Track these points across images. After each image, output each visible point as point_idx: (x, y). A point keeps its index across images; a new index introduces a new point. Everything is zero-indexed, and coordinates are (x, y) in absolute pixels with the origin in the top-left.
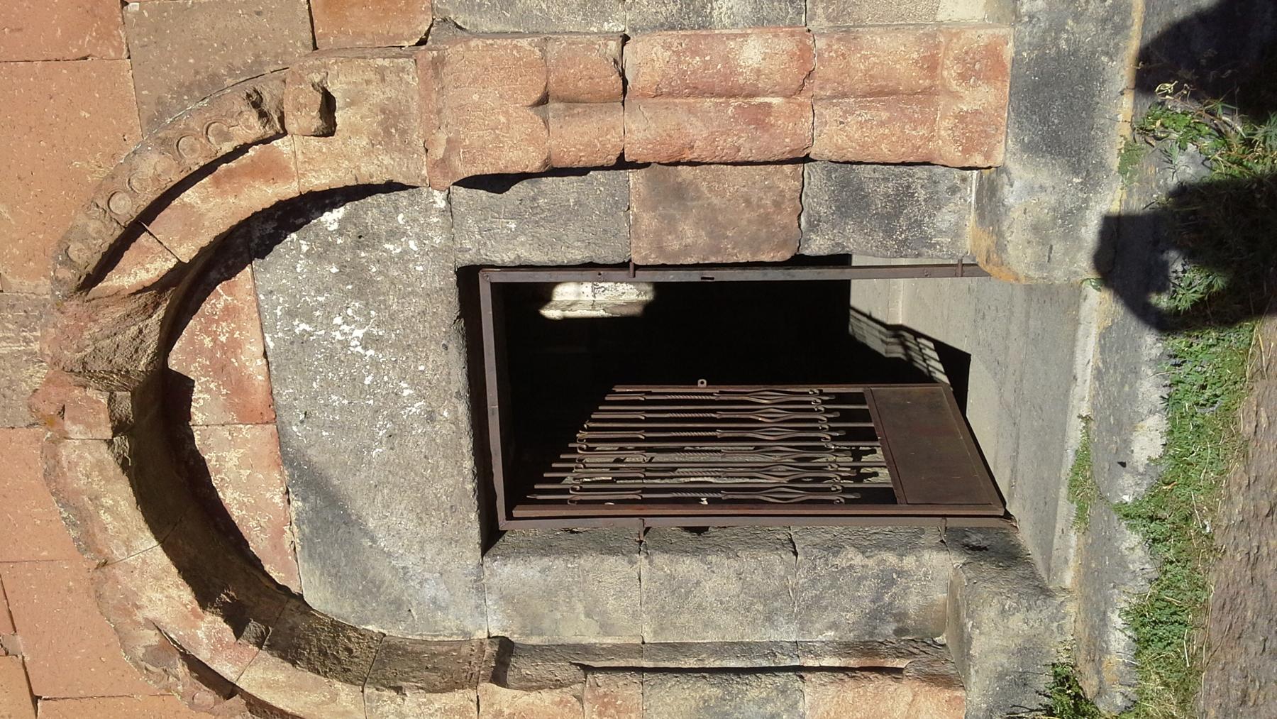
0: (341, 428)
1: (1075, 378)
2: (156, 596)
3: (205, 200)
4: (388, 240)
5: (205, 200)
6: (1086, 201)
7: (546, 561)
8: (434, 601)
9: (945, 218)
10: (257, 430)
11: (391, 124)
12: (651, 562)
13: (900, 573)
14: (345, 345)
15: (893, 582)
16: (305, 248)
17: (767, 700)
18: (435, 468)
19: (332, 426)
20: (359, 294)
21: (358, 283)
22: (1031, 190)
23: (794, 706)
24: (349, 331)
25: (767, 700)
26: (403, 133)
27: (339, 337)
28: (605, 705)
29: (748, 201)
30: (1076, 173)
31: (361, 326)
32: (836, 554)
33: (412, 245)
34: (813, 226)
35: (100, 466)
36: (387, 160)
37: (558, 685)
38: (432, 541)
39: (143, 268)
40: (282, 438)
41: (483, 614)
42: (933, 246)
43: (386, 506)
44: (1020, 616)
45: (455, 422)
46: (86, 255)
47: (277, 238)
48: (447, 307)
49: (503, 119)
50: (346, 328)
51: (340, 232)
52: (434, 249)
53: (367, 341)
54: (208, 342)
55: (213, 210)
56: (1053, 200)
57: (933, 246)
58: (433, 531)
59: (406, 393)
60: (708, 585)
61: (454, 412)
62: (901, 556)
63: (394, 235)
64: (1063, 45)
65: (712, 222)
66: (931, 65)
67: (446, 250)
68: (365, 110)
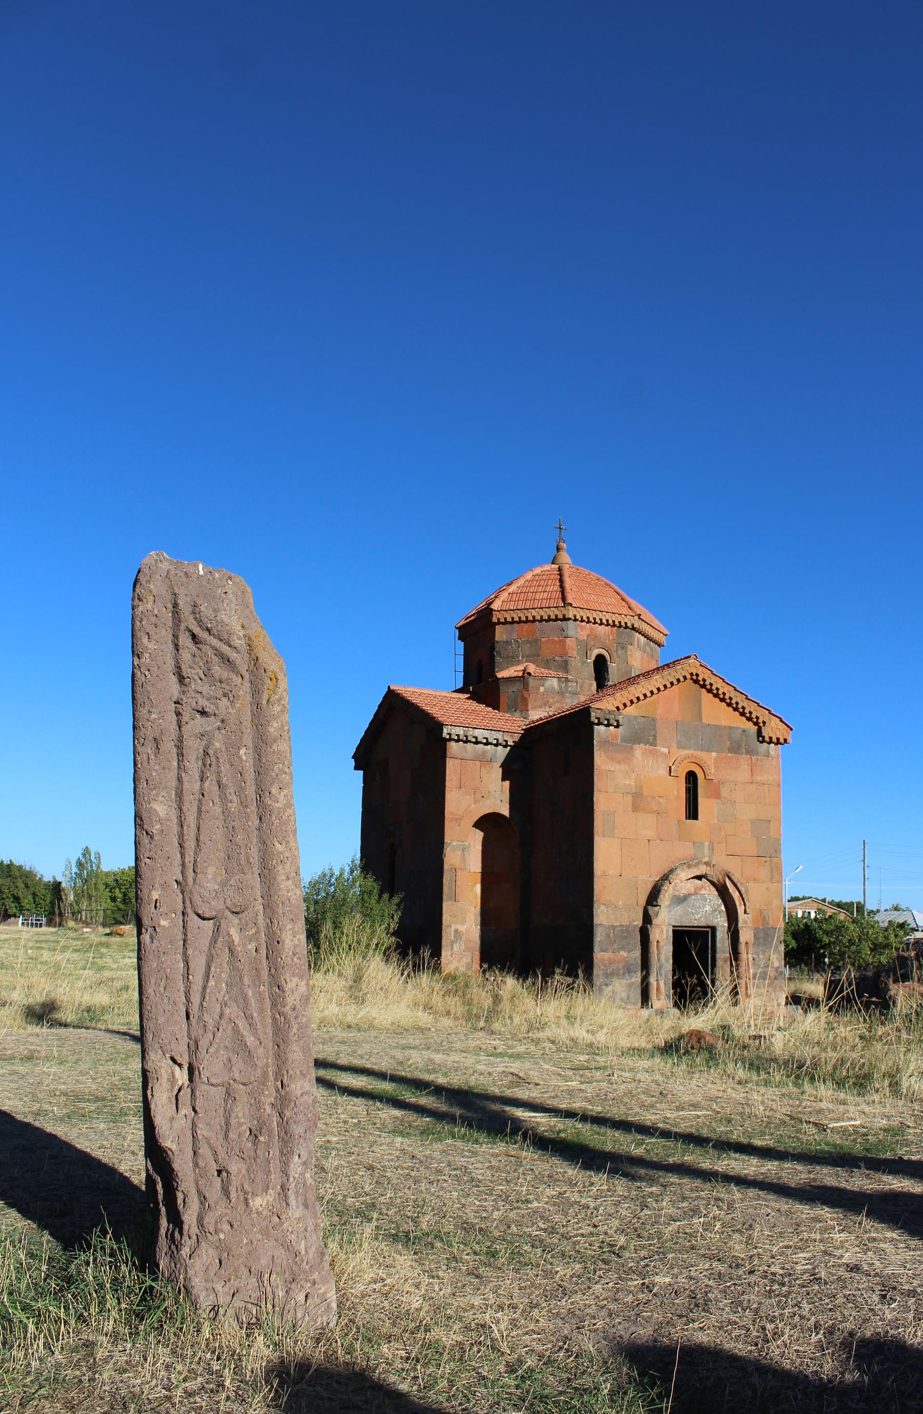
11: (746, 922)
21: (714, 911)
24: (708, 908)
46: (733, 878)
48: (711, 924)
55: (736, 895)
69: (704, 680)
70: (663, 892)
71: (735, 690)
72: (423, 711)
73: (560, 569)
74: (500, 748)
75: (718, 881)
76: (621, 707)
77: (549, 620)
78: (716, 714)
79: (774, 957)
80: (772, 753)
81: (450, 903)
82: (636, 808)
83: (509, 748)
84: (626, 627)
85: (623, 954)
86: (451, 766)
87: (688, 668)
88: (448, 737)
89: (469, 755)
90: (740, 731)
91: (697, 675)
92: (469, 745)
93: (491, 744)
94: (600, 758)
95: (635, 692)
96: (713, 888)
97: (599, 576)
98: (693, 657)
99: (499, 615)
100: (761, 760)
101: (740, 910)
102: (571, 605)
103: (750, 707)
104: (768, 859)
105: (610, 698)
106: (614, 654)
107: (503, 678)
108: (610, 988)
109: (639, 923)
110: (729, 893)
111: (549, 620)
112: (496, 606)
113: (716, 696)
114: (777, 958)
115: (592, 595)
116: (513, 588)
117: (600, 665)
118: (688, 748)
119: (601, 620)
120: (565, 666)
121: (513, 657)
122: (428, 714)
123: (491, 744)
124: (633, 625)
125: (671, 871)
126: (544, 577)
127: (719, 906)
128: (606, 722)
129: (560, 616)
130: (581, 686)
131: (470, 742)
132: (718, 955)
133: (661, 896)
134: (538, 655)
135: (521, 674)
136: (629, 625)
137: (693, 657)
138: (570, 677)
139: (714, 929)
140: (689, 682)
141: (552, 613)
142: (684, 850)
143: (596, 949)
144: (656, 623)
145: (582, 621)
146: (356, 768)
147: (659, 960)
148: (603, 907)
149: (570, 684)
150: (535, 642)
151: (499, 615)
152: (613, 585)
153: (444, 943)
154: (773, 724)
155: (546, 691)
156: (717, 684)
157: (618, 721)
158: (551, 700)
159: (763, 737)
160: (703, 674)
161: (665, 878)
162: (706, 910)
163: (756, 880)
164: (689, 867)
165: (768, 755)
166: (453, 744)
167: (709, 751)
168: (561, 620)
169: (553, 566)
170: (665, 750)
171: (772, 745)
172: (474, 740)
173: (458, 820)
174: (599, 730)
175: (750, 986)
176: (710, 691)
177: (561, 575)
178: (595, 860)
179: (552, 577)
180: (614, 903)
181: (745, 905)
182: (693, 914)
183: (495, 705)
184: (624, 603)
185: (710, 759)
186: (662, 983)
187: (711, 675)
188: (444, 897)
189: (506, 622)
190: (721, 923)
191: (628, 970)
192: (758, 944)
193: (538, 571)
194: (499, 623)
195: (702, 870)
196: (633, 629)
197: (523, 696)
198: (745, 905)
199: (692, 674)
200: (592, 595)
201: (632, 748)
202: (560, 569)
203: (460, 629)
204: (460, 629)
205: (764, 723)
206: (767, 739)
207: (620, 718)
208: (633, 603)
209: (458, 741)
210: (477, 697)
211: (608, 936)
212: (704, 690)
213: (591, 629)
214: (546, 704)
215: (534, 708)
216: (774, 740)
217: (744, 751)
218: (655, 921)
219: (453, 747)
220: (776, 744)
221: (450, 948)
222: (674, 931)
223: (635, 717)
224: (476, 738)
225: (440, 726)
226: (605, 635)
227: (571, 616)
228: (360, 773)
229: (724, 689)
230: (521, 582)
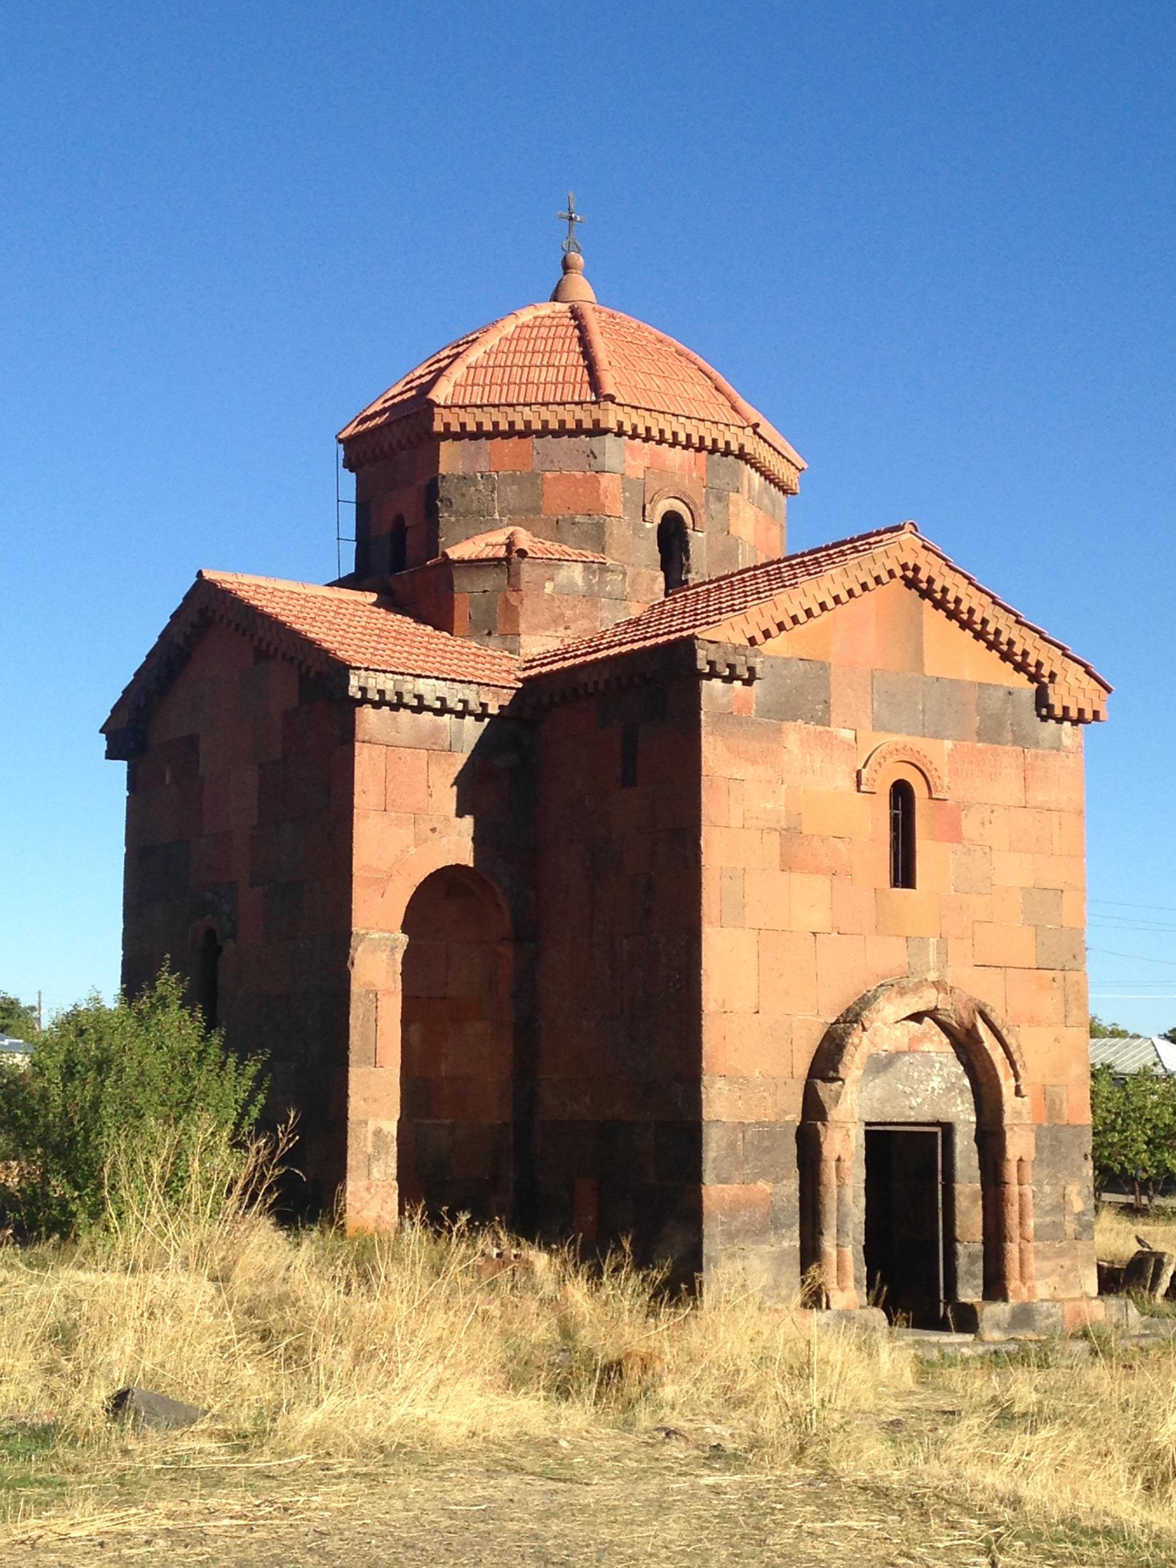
0: (907, 1075)
9: (970, 1292)
11: (1018, 1114)
20: (947, 1088)
22: (1004, 1312)
24: (936, 1082)
33: (960, 1108)
39: (983, 1029)
40: (904, 1053)
46: (992, 1016)
47: (962, 1063)
48: (943, 1118)
55: (997, 1054)
58: (876, 1105)
60: (855, 1210)
61: (913, 1116)
63: (963, 1102)
65: (966, 1213)
66: (1031, 1278)
69: (930, 581)
70: (849, 1049)
71: (995, 602)
72: (296, 633)
73: (576, 314)
74: (469, 719)
75: (961, 1024)
76: (760, 638)
77: (562, 431)
78: (955, 656)
79: (1073, 1190)
80: (1067, 741)
81: (364, 1069)
82: (787, 865)
83: (487, 720)
84: (727, 453)
85: (764, 1186)
86: (367, 764)
87: (898, 553)
88: (359, 695)
89: (404, 737)
90: (1001, 693)
91: (916, 569)
92: (404, 714)
93: (451, 711)
94: (716, 754)
95: (788, 605)
96: (946, 1040)
97: (662, 335)
98: (908, 527)
99: (448, 416)
100: (1043, 758)
101: (1007, 1086)
102: (611, 398)
103: (1024, 641)
104: (1058, 974)
105: (737, 619)
106: (702, 511)
107: (462, 561)
109: (794, 1117)
110: (985, 1050)
111: (562, 431)
112: (441, 393)
113: (952, 615)
114: (1078, 1192)
115: (654, 376)
116: (475, 355)
117: (672, 538)
118: (897, 731)
119: (675, 434)
120: (596, 537)
121: (479, 513)
122: (312, 642)
123: (451, 711)
124: (742, 448)
125: (865, 1002)
126: (544, 332)
127: (958, 1077)
128: (727, 672)
129: (587, 424)
130: (633, 581)
131: (406, 706)
132: (959, 1187)
133: (846, 1058)
134: (537, 510)
135: (502, 553)
136: (734, 447)
137: (908, 527)
138: (609, 562)
139: (948, 1129)
140: (898, 583)
141: (570, 416)
142: (888, 956)
143: (708, 1177)
144: (779, 441)
145: (634, 436)
146: (110, 755)
147: (840, 1200)
148: (720, 1083)
149: (609, 577)
150: (530, 481)
151: (448, 416)
152: (694, 356)
153: (351, 1161)
154: (1070, 679)
155: (559, 591)
156: (957, 588)
157: (751, 670)
158: (568, 613)
159: (1050, 708)
160: (930, 567)
161: (852, 1017)
162: (932, 1089)
163: (1034, 1021)
164: (902, 992)
165: (1058, 747)
166: (367, 710)
167: (936, 736)
168: (590, 433)
169: (558, 306)
170: (848, 735)
171: (1067, 724)
172: (415, 702)
173: (381, 882)
174: (712, 689)
175: (1030, 1257)
176: (939, 605)
177: (582, 328)
178: (704, 979)
179: (561, 331)
180: (744, 1078)
181: (1017, 1076)
182: (907, 1096)
183: (442, 621)
184: (721, 398)
185: (940, 753)
186: (848, 1251)
187: (946, 570)
188: (353, 1057)
189: (463, 434)
190: (963, 1114)
191: (775, 1224)
192: (1041, 1160)
193: (526, 315)
194: (447, 434)
195: (927, 999)
196: (742, 455)
197: (507, 600)
198: (1017, 1076)
199: (904, 567)
200: (654, 376)
201: (780, 730)
202: (576, 314)
203: (348, 443)
204: (348, 443)
205: (1052, 676)
206: (1058, 712)
207: (757, 663)
208: (742, 403)
209: (377, 705)
210: (391, 601)
211: (732, 1145)
212: (928, 603)
213: (654, 455)
214: (557, 620)
215: (534, 629)
216: (1074, 714)
217: (1010, 736)
218: (833, 1114)
219: (369, 719)
220: (1075, 723)
221: (364, 1172)
222: (867, 1132)
223: (787, 660)
224: (420, 697)
225: (343, 669)
226: (681, 468)
227: (613, 425)
228: (122, 766)
229: (971, 600)
230: (491, 340)
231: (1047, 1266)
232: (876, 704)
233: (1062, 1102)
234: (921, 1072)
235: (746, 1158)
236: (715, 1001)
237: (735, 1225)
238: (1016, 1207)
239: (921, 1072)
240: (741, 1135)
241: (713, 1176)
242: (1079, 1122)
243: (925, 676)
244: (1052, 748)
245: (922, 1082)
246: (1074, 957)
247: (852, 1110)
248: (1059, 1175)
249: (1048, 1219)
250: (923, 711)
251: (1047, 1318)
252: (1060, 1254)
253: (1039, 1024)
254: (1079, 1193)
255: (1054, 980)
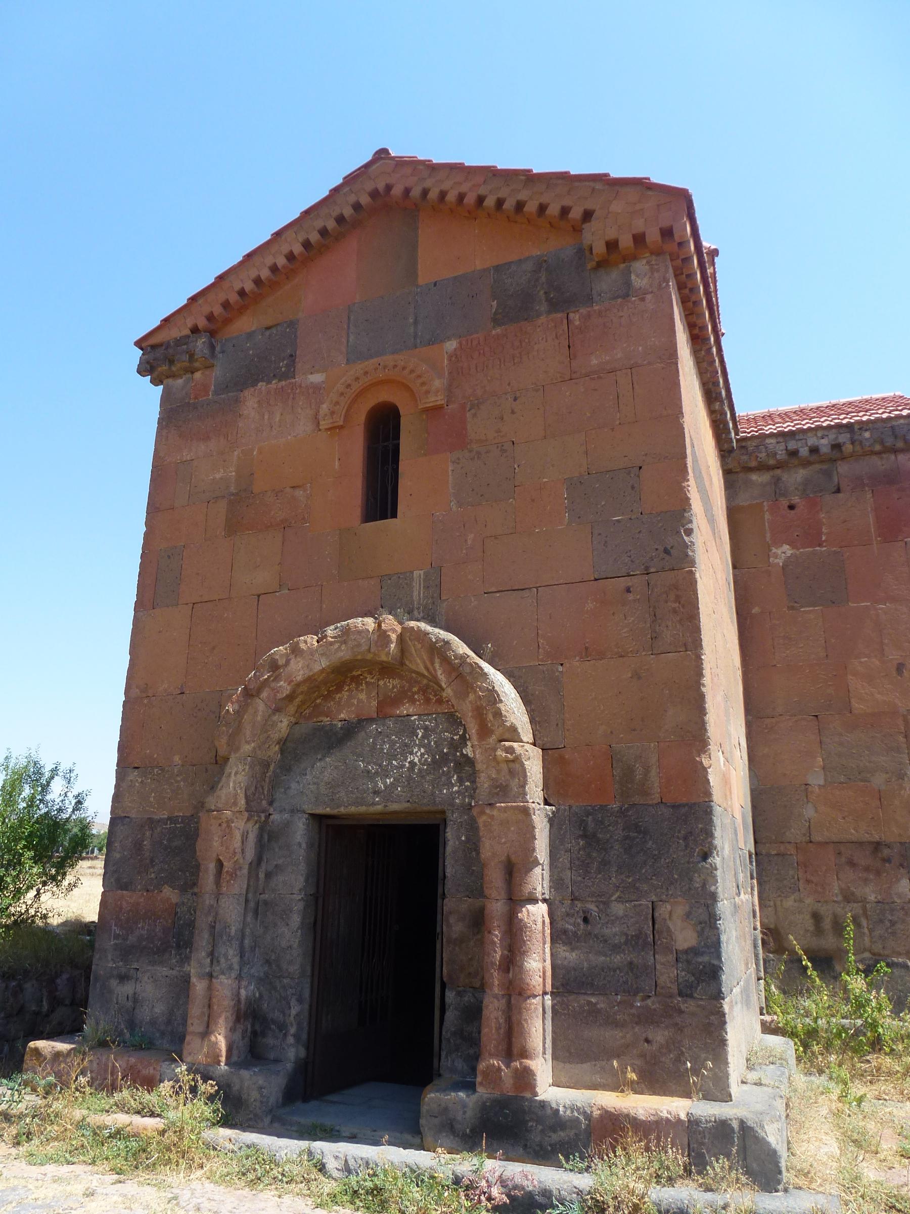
1: (375, 1131)
2: (300, 665)
3: (470, 702)
4: (458, 777)
5: (470, 702)
6: (458, 1136)
7: (304, 845)
8: (289, 788)
10: (374, 709)
12: (300, 900)
13: (285, 1035)
14: (411, 753)
15: (281, 1031)
16: (455, 737)
17: (227, 959)
18: (352, 792)
19: (374, 743)
20: (434, 761)
22: (464, 1106)
23: (223, 973)
24: (417, 756)
25: (227, 959)
26: (497, 794)
27: (415, 751)
28: (231, 875)
29: (471, 959)
30: (471, 1131)
31: (419, 761)
32: (298, 1000)
33: (456, 789)
34: (459, 994)
35: (359, 645)
36: (486, 786)
37: (243, 851)
38: (318, 788)
40: (371, 720)
41: (281, 812)
42: (447, 1057)
43: (336, 768)
44: (258, 1096)
45: (374, 804)
49: (503, 840)
50: (419, 754)
51: (462, 754)
52: (454, 799)
53: (412, 763)
54: (415, 689)
56: (459, 1118)
57: (447, 1057)
59: (388, 780)
62: (294, 1036)
63: (460, 780)
64: (530, 1124)
67: (452, 804)
68: (508, 777)
82: (233, 527)
104: (637, 582)
108: (128, 989)
165: (626, 291)
170: (317, 378)
192: (604, 863)
201: (237, 401)
211: (138, 846)
217: (544, 307)
223: (250, 335)
231: (613, 1036)
232: (352, 338)
233: (647, 770)
234: (393, 744)
235: (152, 861)
236: (137, 687)
237: (132, 939)
238: (497, 935)
239: (395, 743)
240: (148, 833)
241: (112, 880)
242: (684, 800)
243: (418, 286)
244: (618, 297)
245: (395, 757)
246: (666, 551)
247: (236, 795)
248: (645, 887)
249: (618, 959)
250: (416, 323)
251: (553, 1129)
252: (647, 1018)
253: (601, 655)
254: (688, 915)
255: (628, 590)
